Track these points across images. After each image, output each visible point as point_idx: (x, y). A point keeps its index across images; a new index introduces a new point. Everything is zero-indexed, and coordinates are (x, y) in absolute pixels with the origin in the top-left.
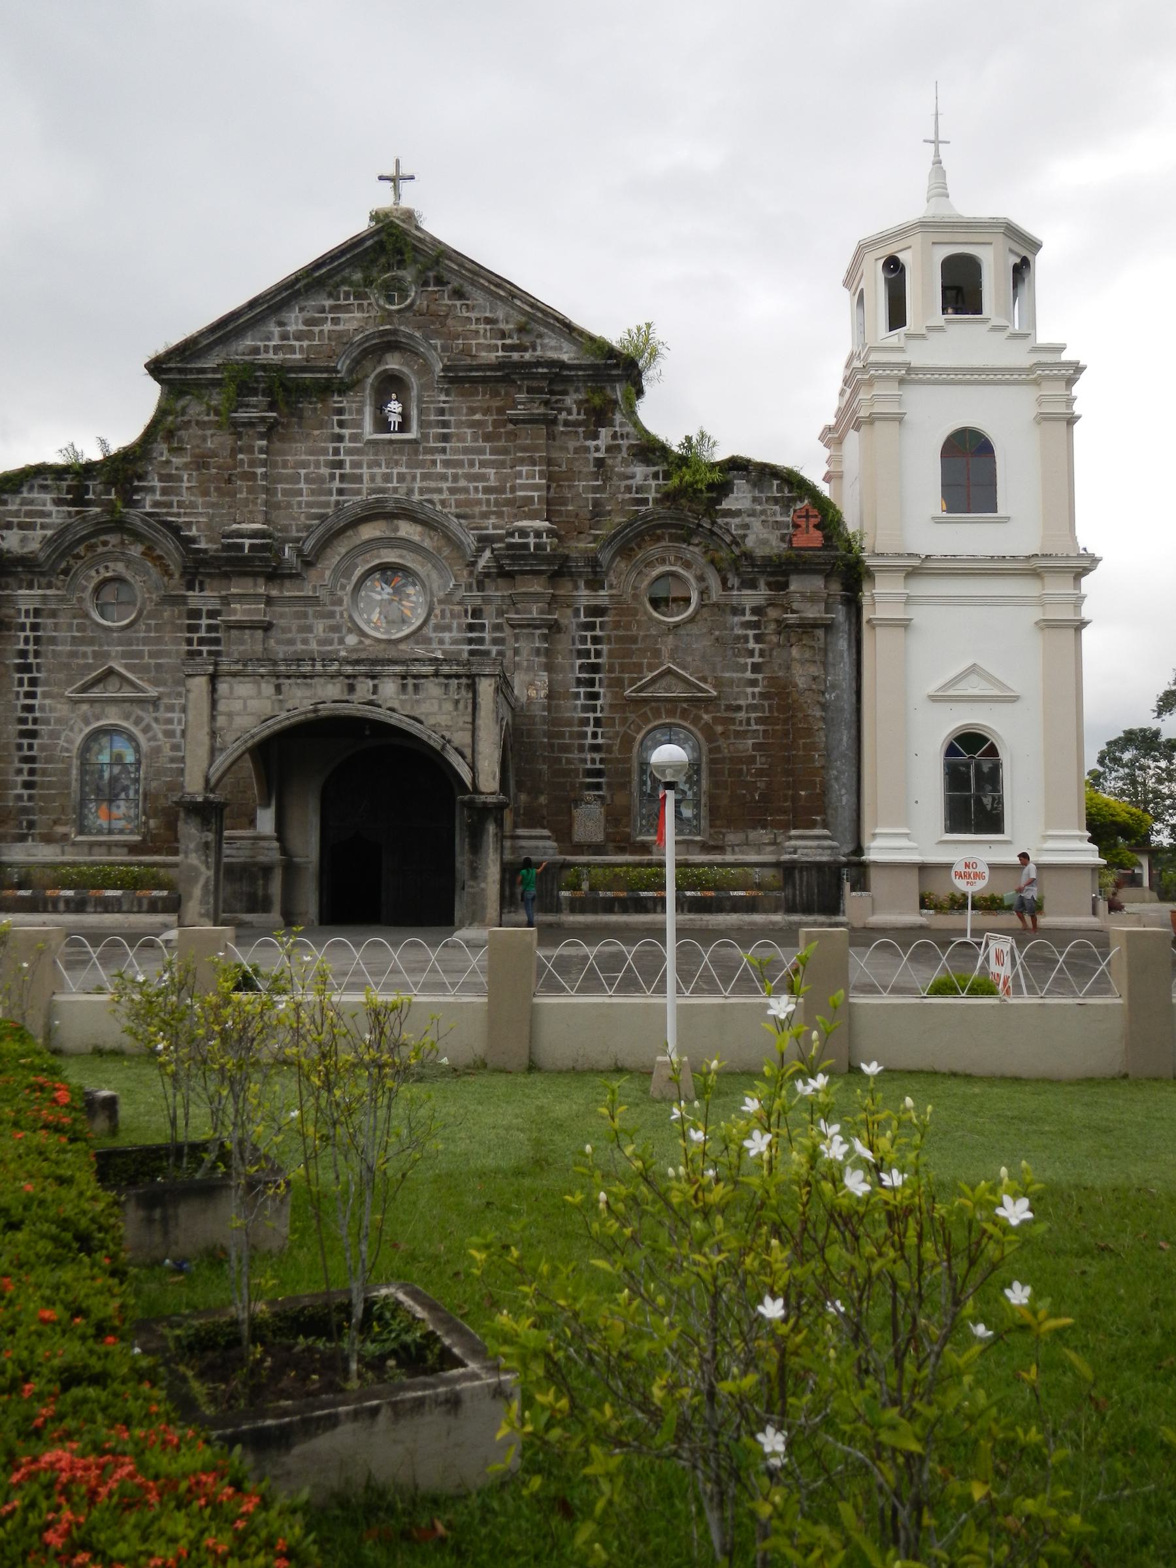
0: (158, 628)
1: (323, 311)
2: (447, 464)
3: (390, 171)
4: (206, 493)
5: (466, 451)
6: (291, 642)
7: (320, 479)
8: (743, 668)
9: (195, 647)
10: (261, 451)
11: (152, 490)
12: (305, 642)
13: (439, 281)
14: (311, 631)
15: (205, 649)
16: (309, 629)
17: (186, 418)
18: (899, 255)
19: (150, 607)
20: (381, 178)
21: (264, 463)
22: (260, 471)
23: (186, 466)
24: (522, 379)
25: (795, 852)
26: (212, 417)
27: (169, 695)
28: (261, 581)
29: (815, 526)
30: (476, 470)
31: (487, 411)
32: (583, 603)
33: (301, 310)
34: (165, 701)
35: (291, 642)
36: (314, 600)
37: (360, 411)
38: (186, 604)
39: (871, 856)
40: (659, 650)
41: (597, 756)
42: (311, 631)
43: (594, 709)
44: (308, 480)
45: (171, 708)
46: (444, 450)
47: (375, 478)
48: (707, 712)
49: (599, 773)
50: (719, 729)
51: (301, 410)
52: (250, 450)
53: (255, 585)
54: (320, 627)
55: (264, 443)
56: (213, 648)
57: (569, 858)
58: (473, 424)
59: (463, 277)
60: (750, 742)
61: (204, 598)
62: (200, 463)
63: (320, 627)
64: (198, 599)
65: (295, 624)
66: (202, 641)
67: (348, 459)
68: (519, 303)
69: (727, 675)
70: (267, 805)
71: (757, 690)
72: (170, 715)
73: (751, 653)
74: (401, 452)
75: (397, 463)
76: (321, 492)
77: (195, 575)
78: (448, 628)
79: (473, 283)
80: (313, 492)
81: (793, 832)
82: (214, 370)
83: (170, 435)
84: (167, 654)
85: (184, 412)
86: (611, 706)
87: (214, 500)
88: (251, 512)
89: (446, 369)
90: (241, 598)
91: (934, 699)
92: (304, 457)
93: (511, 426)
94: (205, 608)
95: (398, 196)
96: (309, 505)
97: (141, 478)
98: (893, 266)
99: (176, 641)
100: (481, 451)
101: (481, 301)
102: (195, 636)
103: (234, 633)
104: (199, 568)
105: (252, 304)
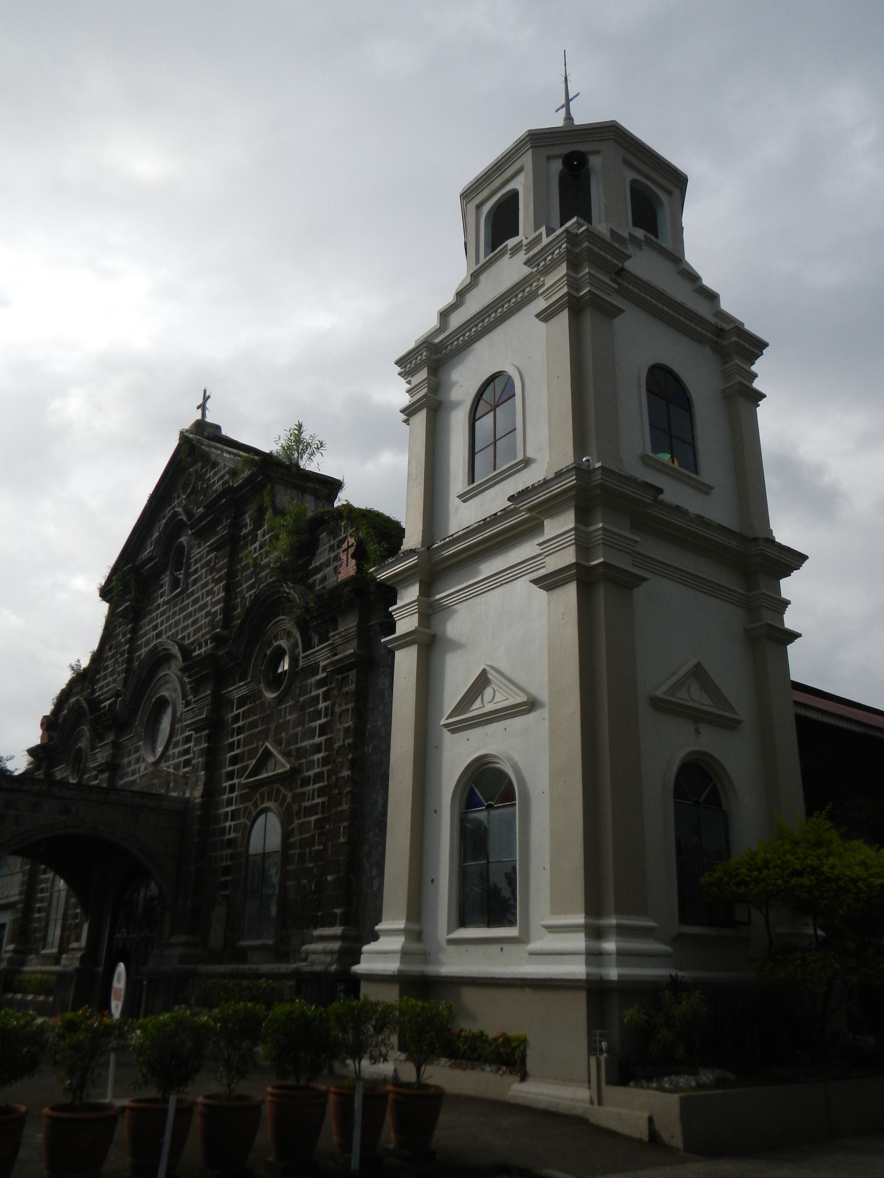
8: (311, 734)
20: (198, 408)
25: (305, 960)
29: (353, 556)
32: (236, 695)
39: (364, 966)
40: (268, 729)
41: (229, 852)
43: (230, 802)
48: (290, 791)
49: (227, 871)
50: (295, 807)
57: (203, 968)
60: (313, 818)
69: (304, 744)
71: (320, 755)
73: (317, 715)
74: (175, 605)
78: (176, 745)
81: (318, 932)
86: (241, 796)
91: (455, 728)
95: (204, 415)
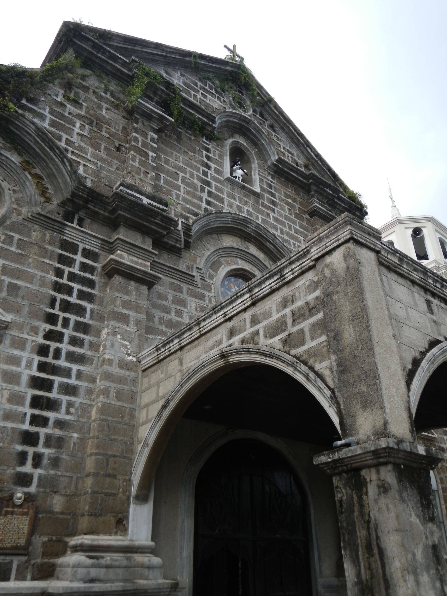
0: (21, 244)
1: (197, 86)
2: (276, 219)
3: (232, 48)
4: (96, 147)
5: (286, 218)
6: (167, 310)
7: (194, 187)
9: (64, 281)
10: (153, 140)
11: (42, 117)
12: (179, 313)
13: (261, 115)
14: (185, 306)
15: (76, 287)
16: (183, 303)
17: (84, 83)
18: (422, 229)
19: (14, 218)
21: (154, 150)
22: (151, 154)
23: (79, 116)
24: (316, 191)
26: (108, 96)
27: (21, 327)
28: (149, 241)
30: (292, 232)
31: (294, 200)
33: (182, 75)
34: (14, 332)
35: (167, 310)
36: (188, 278)
37: (221, 156)
38: (62, 232)
42: (185, 306)
44: (183, 182)
45: (20, 344)
46: (273, 211)
47: (232, 205)
51: (180, 133)
52: (145, 135)
53: (144, 242)
54: (192, 304)
55: (156, 136)
56: (85, 289)
58: (288, 204)
59: (277, 120)
61: (84, 235)
62: (95, 122)
63: (192, 304)
64: (72, 232)
65: (171, 294)
66: (72, 277)
67: (214, 183)
68: (309, 151)
70: (142, 498)
72: (16, 352)
75: (246, 203)
76: (195, 196)
77: (78, 208)
79: (282, 128)
80: (187, 193)
82: (124, 64)
83: (68, 86)
84: (30, 278)
85: (84, 77)
87: (104, 156)
88: (141, 180)
89: (280, 161)
90: (132, 248)
92: (181, 164)
93: (308, 217)
94: (81, 246)
96: (184, 199)
97: (30, 100)
98: (417, 232)
99: (42, 267)
100: (294, 223)
101: (284, 140)
102: (67, 270)
103: (117, 279)
104: (85, 204)
105: (158, 46)
